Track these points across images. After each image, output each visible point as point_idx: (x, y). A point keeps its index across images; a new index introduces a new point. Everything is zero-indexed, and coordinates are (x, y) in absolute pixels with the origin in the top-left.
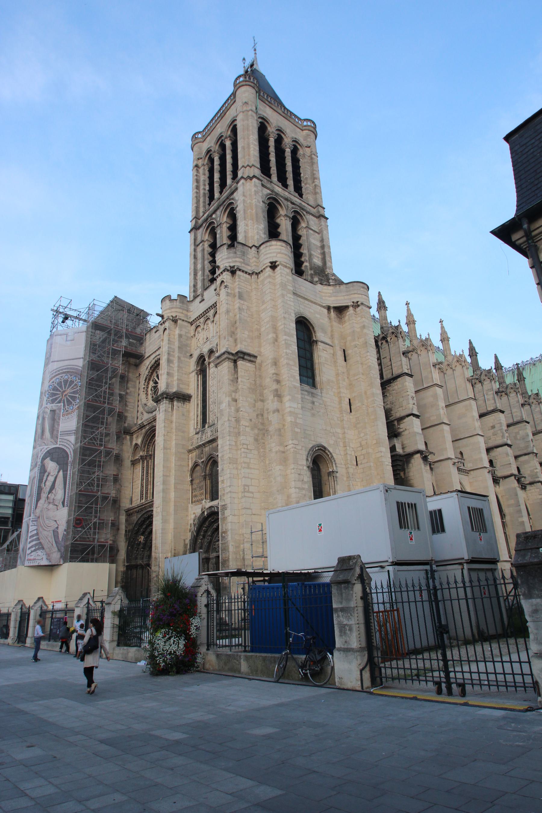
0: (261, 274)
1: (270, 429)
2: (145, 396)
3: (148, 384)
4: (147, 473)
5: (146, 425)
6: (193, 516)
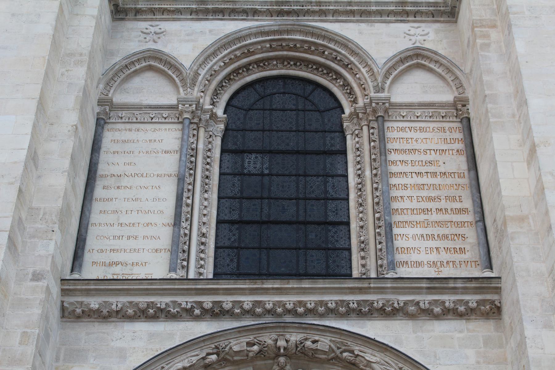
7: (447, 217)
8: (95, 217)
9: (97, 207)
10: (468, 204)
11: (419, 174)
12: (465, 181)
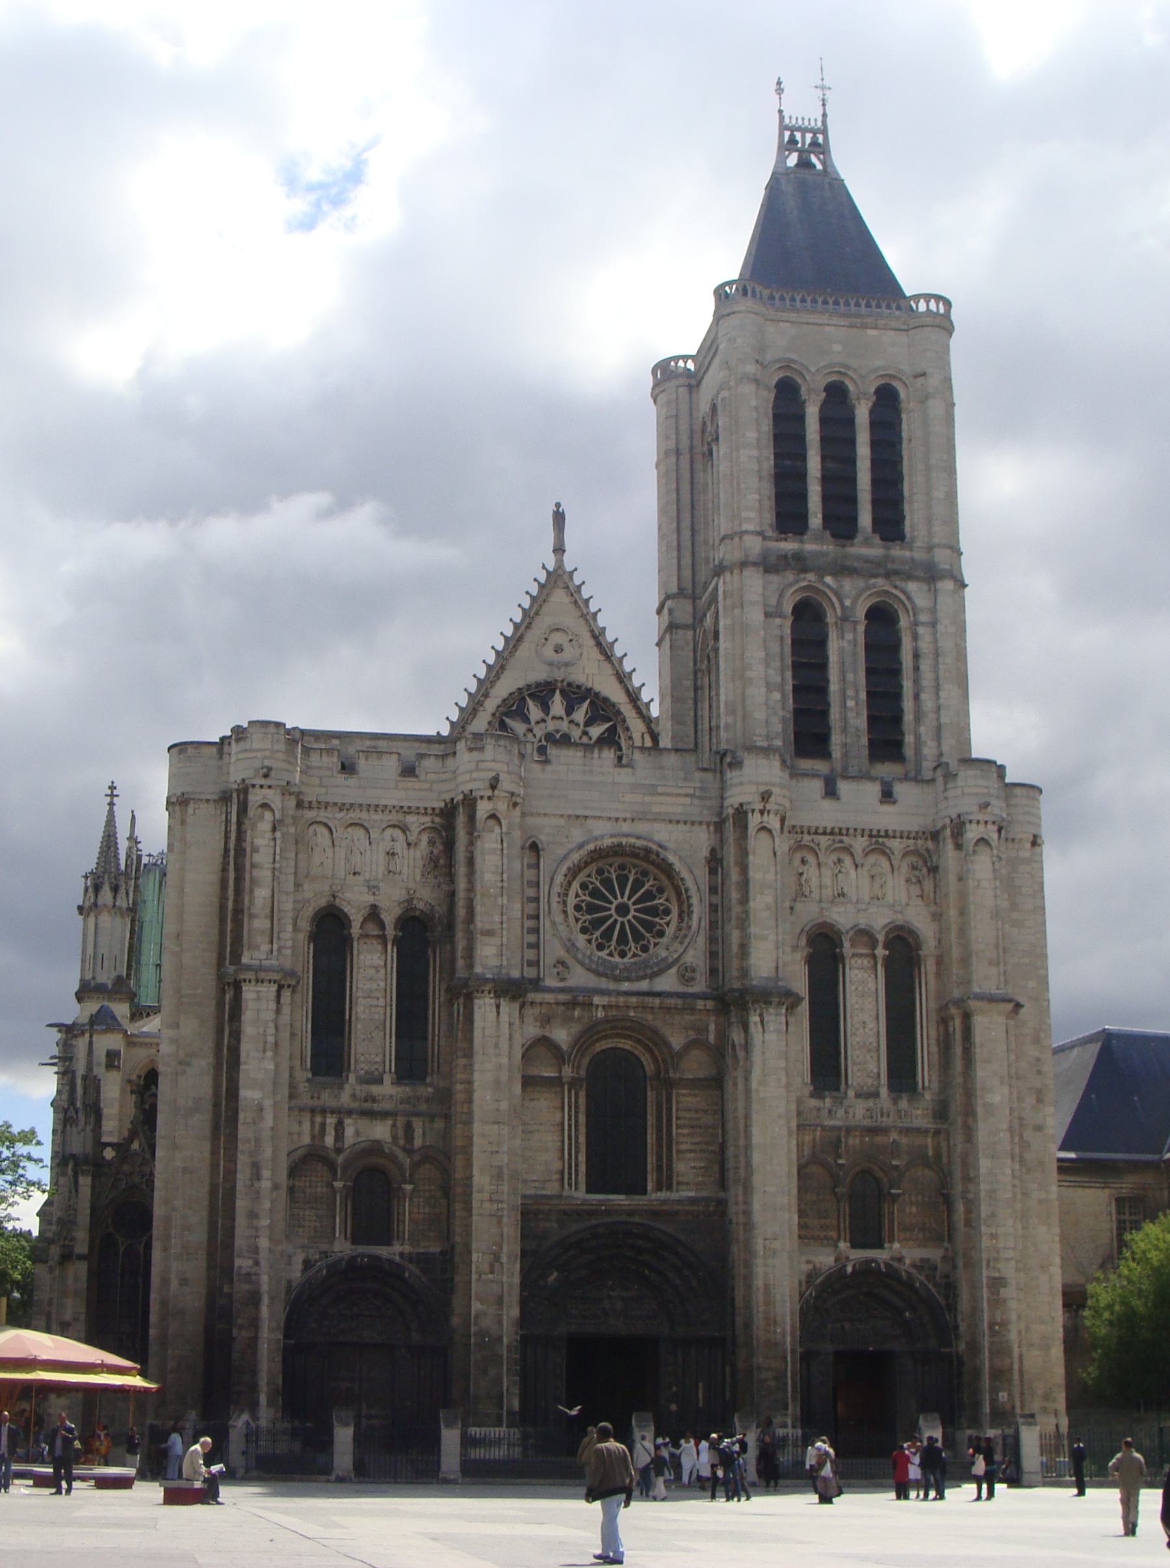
0: (1010, 845)
1: (1027, 1156)
2: (562, 916)
3: (570, 884)
4: (576, 1122)
5: (597, 1006)
6: (806, 1268)
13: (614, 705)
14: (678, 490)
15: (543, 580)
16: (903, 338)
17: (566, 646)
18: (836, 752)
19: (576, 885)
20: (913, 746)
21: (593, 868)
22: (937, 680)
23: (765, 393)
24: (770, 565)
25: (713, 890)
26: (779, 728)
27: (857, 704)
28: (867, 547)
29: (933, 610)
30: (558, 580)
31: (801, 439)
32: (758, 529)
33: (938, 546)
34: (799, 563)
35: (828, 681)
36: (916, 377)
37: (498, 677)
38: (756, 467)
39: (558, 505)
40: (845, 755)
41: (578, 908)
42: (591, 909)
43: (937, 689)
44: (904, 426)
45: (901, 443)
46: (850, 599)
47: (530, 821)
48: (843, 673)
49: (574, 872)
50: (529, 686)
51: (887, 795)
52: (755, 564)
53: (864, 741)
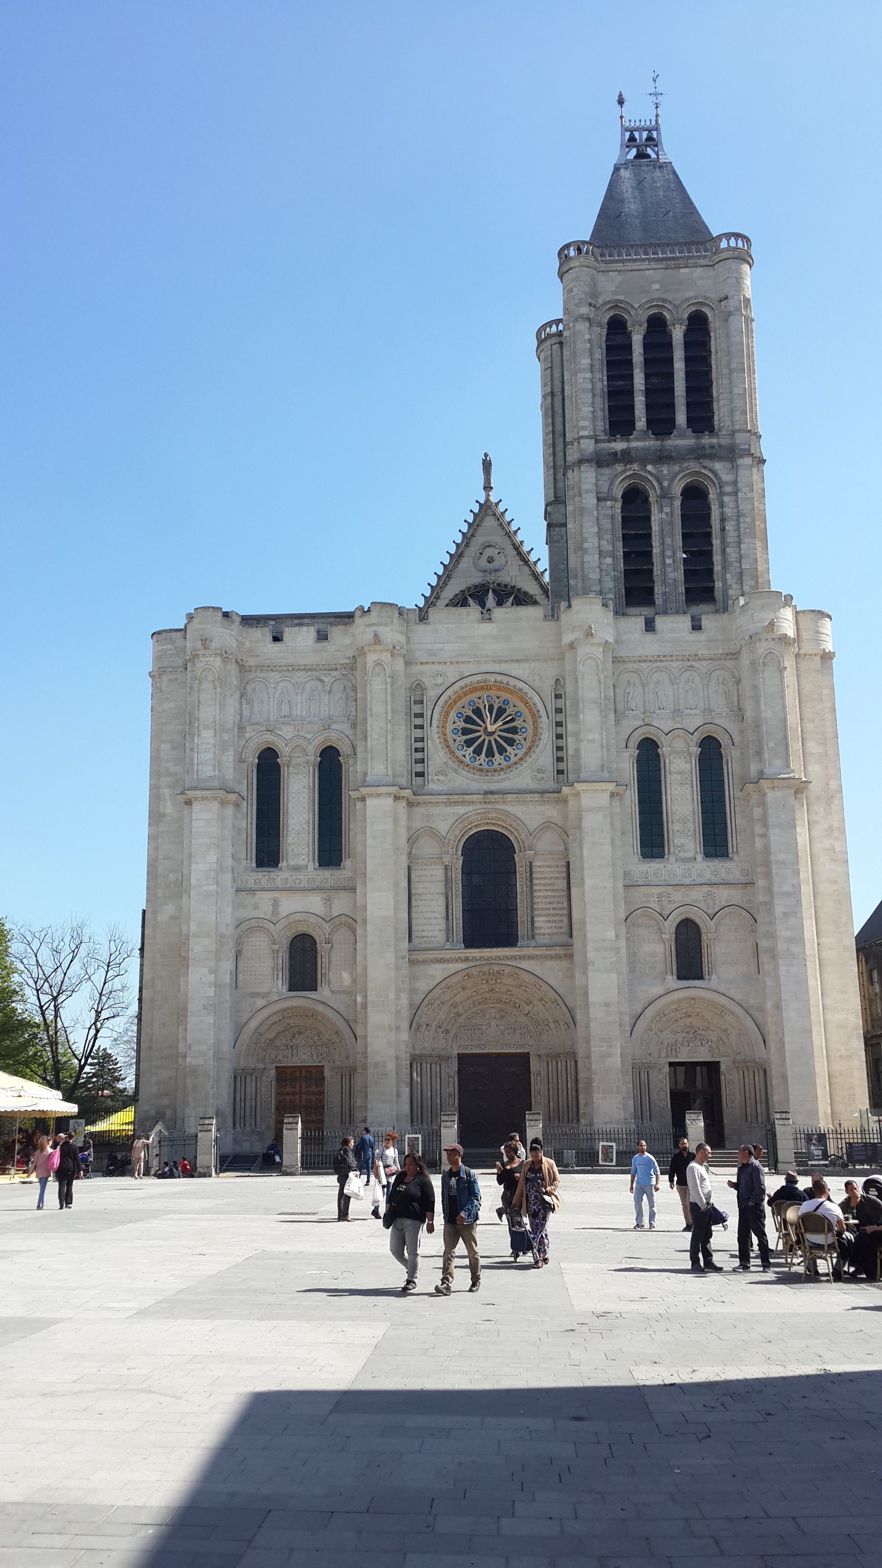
7: (557, 912)
8: (414, 915)
9: (414, 910)
10: (565, 905)
11: (546, 890)
12: (565, 893)
13: (531, 597)
14: (553, 424)
15: (476, 511)
16: (710, 272)
17: (496, 557)
18: (659, 600)
19: (453, 715)
20: (721, 590)
21: (465, 700)
22: (739, 536)
23: (597, 329)
24: (600, 461)
25: (559, 711)
26: (611, 585)
27: (674, 562)
28: (682, 440)
29: (735, 483)
30: (487, 510)
31: (629, 363)
32: (592, 434)
33: (739, 431)
34: (625, 457)
35: (651, 546)
36: (721, 301)
37: (445, 584)
38: (589, 386)
39: (486, 455)
40: (665, 601)
41: (455, 731)
42: (465, 731)
43: (739, 543)
44: (713, 343)
45: (710, 355)
46: (667, 484)
47: (417, 668)
48: (662, 537)
49: (450, 705)
50: (469, 588)
51: (697, 627)
52: (588, 461)
53: (682, 589)
